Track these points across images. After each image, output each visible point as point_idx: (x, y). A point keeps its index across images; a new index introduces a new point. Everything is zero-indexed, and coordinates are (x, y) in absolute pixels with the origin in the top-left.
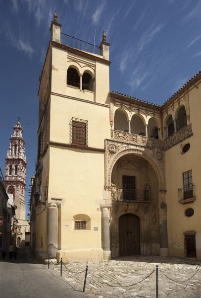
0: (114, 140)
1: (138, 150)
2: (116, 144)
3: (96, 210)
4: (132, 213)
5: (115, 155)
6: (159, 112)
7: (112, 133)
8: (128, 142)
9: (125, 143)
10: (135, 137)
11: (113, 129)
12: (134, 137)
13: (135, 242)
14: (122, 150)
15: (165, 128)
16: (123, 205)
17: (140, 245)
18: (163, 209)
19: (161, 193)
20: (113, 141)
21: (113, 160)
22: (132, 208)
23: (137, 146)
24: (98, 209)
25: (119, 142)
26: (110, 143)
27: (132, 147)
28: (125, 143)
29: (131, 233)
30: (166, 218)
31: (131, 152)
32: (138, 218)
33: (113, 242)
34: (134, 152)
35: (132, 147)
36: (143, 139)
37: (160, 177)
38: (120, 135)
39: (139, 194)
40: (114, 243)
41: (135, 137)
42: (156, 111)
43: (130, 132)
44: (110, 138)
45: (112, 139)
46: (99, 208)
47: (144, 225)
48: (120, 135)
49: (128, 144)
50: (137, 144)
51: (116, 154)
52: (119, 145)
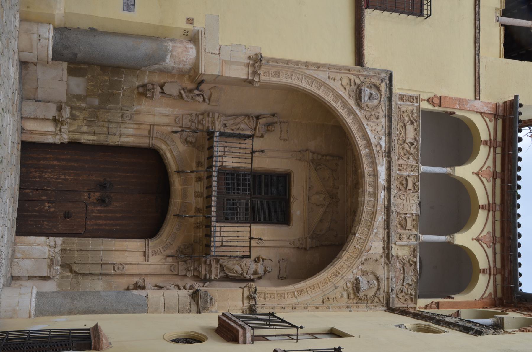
0: (393, 104)
1: (375, 195)
2: (382, 111)
3: (191, 16)
4: (172, 200)
5: (352, 102)
6: (499, 295)
7: (412, 99)
8: (394, 157)
9: (390, 142)
10: (410, 186)
11: (425, 106)
12: (410, 181)
13: (67, 215)
14: (370, 131)
15: (458, 314)
16: (199, 164)
17: (56, 235)
18: (188, 299)
19: (246, 293)
20: (390, 99)
21: (336, 94)
22: (184, 192)
23: (388, 189)
24: (190, 21)
25: (390, 121)
26: (383, 87)
27: (382, 170)
28: (390, 142)
29: (101, 201)
30: (156, 310)
31: (367, 169)
32: (149, 231)
33: (76, 113)
34: (368, 180)
35: (382, 170)
36: (409, 221)
37: (301, 292)
38: (410, 128)
39: (229, 236)
40: (73, 117)
41: (410, 186)
42: (499, 277)
43: (423, 169)
44: (397, 90)
45: (395, 99)
46: (199, 25)
47: (128, 253)
48: (410, 128)
49: (388, 153)
50: (393, 193)
51: (355, 108)
52: (383, 121)
